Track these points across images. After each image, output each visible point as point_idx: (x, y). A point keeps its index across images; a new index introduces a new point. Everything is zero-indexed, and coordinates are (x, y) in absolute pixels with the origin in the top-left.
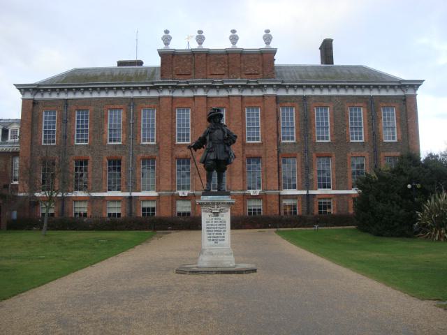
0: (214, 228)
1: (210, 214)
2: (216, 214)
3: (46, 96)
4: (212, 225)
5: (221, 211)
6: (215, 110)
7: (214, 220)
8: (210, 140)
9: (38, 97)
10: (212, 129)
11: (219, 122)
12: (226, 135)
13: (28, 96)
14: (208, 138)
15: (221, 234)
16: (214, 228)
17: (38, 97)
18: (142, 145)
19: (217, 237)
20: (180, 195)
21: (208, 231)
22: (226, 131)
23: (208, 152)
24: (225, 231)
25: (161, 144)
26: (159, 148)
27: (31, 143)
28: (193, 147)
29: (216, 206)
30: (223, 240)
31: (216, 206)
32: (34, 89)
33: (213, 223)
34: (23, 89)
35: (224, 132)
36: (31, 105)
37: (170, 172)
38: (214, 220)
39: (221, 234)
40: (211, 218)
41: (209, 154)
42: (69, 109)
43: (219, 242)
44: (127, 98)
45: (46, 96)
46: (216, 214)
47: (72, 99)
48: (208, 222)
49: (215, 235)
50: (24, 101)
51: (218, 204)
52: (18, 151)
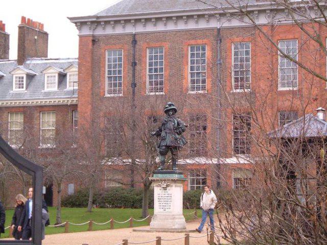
2: (165, 189)
3: (109, 31)
5: (167, 186)
7: (163, 193)
9: (99, 32)
13: (87, 31)
17: (99, 32)
27: (92, 94)
32: (92, 22)
34: (80, 23)
36: (91, 44)
38: (163, 193)
42: (137, 46)
44: (212, 29)
45: (109, 31)
46: (165, 189)
47: (142, 34)
48: (159, 194)
50: (81, 37)
51: (165, 180)
52: (74, 102)
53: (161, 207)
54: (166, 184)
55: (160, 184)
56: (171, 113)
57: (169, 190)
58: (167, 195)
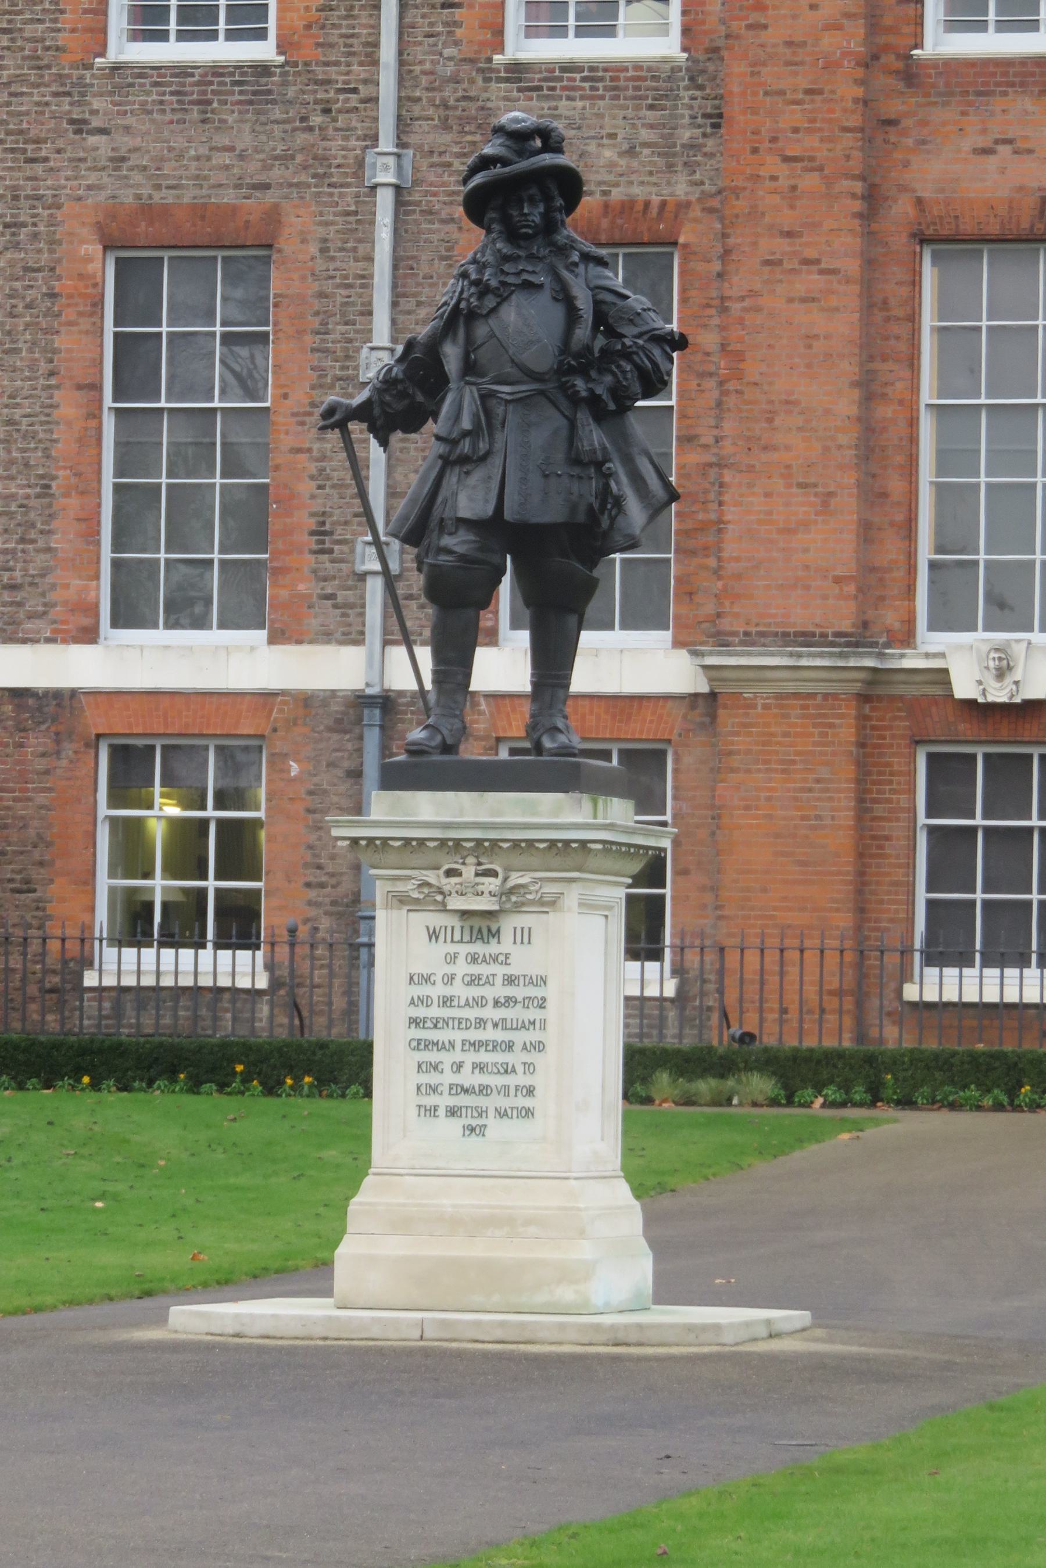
0: (462, 1024)
1: (437, 920)
4: (447, 1001)
6: (519, 138)
7: (462, 968)
8: (470, 368)
10: (483, 290)
11: (550, 227)
12: (582, 333)
14: (452, 355)
15: (508, 1070)
16: (462, 1024)
18: (517, 70)
19: (484, 1090)
20: (964, 688)
21: (420, 1045)
22: (584, 302)
23: (447, 463)
24: (539, 1047)
25: (736, 69)
26: (716, 120)
28: (362, 413)
29: (469, 872)
30: (528, 1113)
31: (469, 872)
33: (460, 991)
35: (572, 315)
37: (847, 405)
38: (462, 968)
39: (508, 1070)
40: (443, 948)
41: (452, 478)
43: (495, 1127)
48: (427, 979)
49: (469, 1078)
53: (445, 1101)
54: (491, 884)
55: (431, 877)
56: (535, 214)
57: (525, 936)
58: (501, 991)
